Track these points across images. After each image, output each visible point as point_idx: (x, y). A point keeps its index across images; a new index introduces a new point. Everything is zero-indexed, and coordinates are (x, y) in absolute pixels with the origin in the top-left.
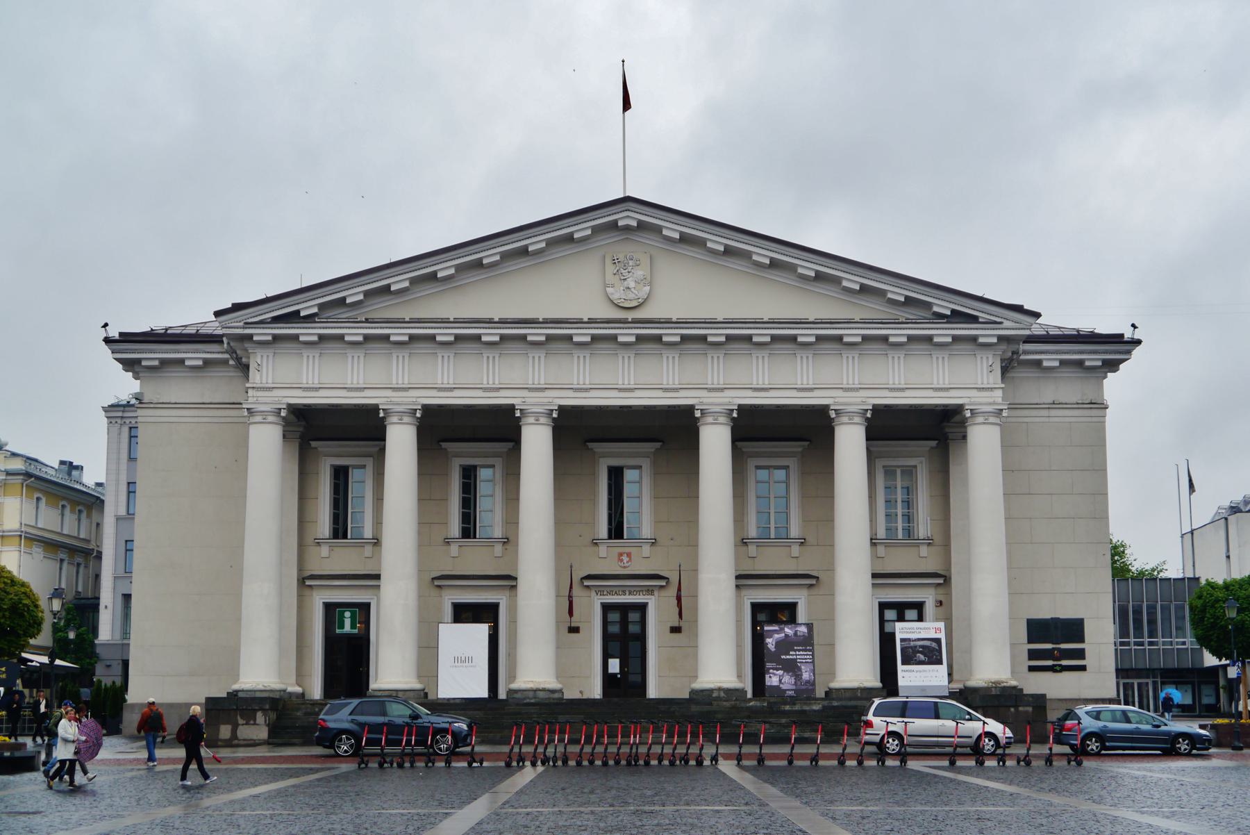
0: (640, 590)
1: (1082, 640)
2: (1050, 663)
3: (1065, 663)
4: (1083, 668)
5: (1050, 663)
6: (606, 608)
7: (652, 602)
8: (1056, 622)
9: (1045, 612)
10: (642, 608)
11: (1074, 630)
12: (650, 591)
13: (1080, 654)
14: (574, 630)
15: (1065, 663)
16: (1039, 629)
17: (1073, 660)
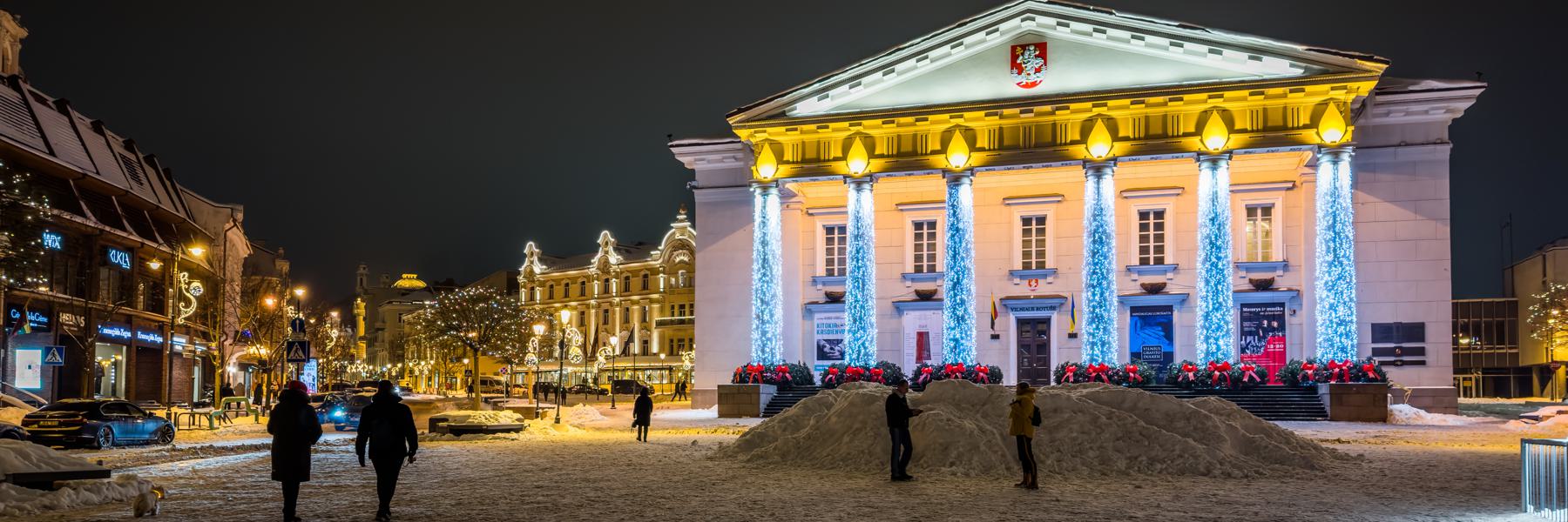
0: (1044, 308)
1: (1423, 340)
2: (1392, 359)
3: (1405, 358)
4: (1423, 363)
5: (1392, 359)
6: (1021, 323)
7: (1055, 317)
8: (1399, 325)
9: (1389, 320)
10: (1047, 321)
11: (1415, 331)
12: (1053, 308)
13: (1422, 351)
14: (995, 337)
15: (1405, 358)
16: (1381, 332)
17: (1417, 357)
